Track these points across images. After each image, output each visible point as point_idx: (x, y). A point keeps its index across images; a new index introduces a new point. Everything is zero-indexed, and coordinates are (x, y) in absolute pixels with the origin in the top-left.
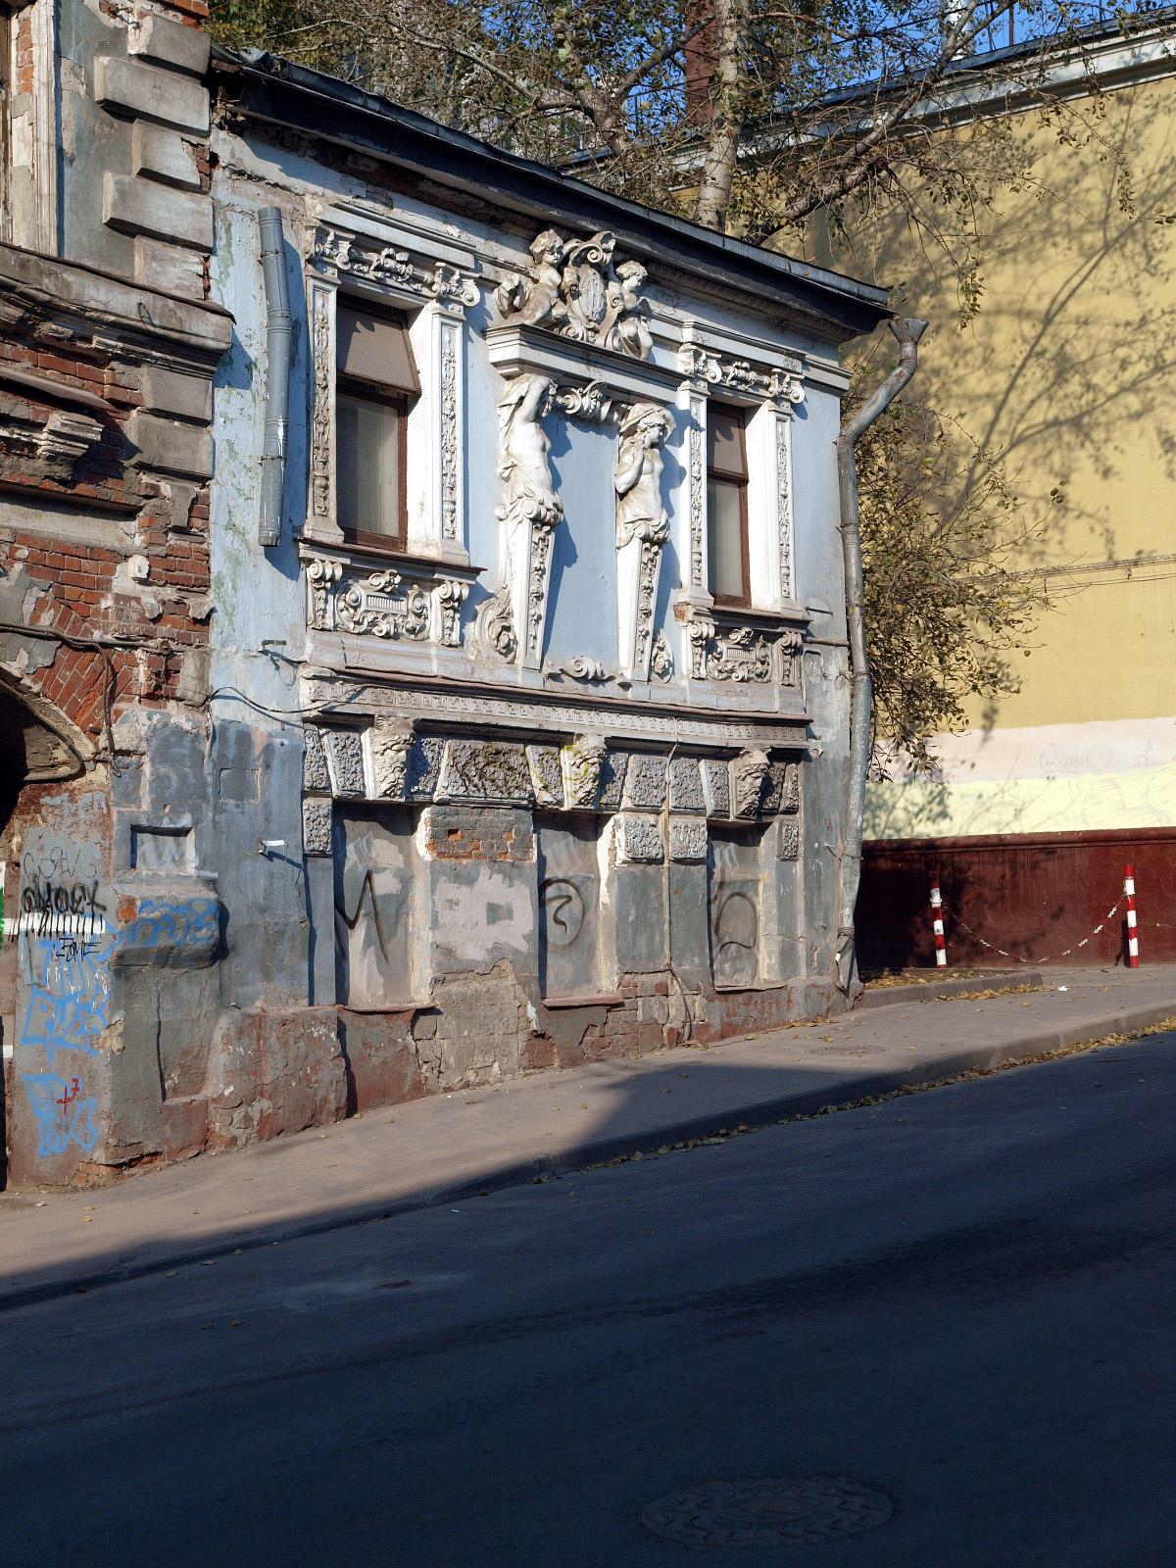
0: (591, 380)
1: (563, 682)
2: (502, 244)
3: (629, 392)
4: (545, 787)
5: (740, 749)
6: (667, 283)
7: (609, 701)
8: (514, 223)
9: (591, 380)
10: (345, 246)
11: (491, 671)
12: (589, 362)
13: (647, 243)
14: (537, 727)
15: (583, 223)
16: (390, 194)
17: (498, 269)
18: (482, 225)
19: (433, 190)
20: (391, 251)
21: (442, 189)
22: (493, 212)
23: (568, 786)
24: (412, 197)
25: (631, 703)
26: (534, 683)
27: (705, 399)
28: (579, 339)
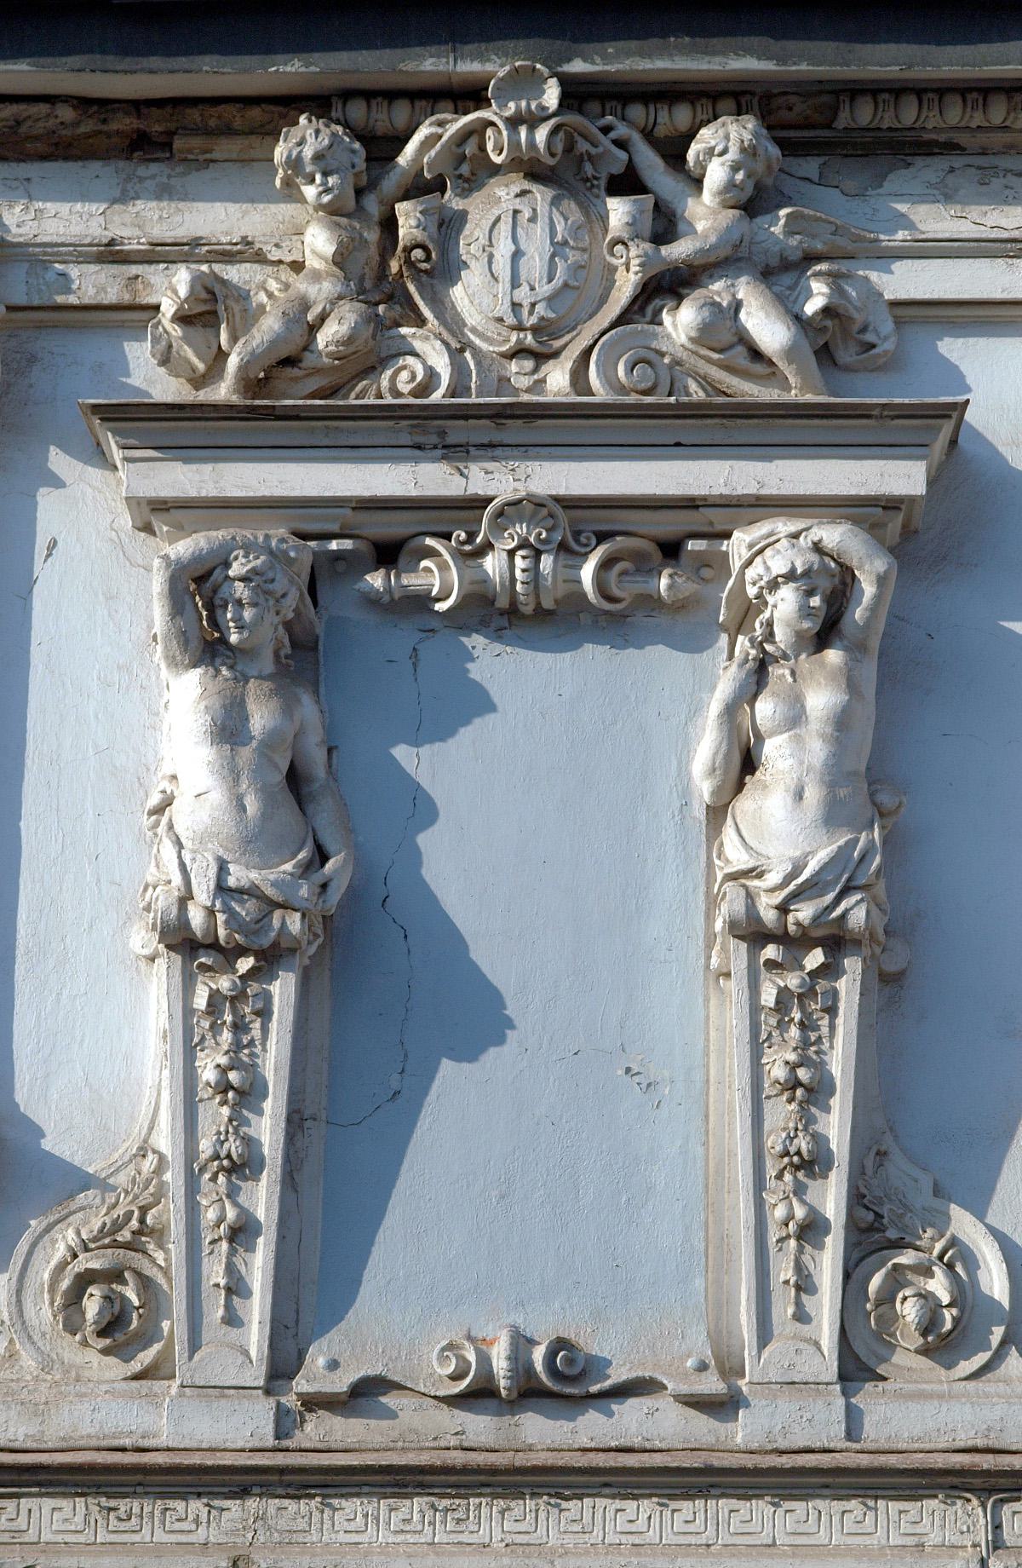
0: (490, 500)
1: (392, 1415)
2: (185, 198)
3: (691, 504)
6: (982, 139)
7: (986, 1462)
8: (228, 131)
9: (490, 500)
11: (38, 1411)
12: (455, 452)
13: (749, 51)
17: (134, 269)
18: (95, 166)
22: (124, 123)
25: (749, 1461)
28: (437, 397)
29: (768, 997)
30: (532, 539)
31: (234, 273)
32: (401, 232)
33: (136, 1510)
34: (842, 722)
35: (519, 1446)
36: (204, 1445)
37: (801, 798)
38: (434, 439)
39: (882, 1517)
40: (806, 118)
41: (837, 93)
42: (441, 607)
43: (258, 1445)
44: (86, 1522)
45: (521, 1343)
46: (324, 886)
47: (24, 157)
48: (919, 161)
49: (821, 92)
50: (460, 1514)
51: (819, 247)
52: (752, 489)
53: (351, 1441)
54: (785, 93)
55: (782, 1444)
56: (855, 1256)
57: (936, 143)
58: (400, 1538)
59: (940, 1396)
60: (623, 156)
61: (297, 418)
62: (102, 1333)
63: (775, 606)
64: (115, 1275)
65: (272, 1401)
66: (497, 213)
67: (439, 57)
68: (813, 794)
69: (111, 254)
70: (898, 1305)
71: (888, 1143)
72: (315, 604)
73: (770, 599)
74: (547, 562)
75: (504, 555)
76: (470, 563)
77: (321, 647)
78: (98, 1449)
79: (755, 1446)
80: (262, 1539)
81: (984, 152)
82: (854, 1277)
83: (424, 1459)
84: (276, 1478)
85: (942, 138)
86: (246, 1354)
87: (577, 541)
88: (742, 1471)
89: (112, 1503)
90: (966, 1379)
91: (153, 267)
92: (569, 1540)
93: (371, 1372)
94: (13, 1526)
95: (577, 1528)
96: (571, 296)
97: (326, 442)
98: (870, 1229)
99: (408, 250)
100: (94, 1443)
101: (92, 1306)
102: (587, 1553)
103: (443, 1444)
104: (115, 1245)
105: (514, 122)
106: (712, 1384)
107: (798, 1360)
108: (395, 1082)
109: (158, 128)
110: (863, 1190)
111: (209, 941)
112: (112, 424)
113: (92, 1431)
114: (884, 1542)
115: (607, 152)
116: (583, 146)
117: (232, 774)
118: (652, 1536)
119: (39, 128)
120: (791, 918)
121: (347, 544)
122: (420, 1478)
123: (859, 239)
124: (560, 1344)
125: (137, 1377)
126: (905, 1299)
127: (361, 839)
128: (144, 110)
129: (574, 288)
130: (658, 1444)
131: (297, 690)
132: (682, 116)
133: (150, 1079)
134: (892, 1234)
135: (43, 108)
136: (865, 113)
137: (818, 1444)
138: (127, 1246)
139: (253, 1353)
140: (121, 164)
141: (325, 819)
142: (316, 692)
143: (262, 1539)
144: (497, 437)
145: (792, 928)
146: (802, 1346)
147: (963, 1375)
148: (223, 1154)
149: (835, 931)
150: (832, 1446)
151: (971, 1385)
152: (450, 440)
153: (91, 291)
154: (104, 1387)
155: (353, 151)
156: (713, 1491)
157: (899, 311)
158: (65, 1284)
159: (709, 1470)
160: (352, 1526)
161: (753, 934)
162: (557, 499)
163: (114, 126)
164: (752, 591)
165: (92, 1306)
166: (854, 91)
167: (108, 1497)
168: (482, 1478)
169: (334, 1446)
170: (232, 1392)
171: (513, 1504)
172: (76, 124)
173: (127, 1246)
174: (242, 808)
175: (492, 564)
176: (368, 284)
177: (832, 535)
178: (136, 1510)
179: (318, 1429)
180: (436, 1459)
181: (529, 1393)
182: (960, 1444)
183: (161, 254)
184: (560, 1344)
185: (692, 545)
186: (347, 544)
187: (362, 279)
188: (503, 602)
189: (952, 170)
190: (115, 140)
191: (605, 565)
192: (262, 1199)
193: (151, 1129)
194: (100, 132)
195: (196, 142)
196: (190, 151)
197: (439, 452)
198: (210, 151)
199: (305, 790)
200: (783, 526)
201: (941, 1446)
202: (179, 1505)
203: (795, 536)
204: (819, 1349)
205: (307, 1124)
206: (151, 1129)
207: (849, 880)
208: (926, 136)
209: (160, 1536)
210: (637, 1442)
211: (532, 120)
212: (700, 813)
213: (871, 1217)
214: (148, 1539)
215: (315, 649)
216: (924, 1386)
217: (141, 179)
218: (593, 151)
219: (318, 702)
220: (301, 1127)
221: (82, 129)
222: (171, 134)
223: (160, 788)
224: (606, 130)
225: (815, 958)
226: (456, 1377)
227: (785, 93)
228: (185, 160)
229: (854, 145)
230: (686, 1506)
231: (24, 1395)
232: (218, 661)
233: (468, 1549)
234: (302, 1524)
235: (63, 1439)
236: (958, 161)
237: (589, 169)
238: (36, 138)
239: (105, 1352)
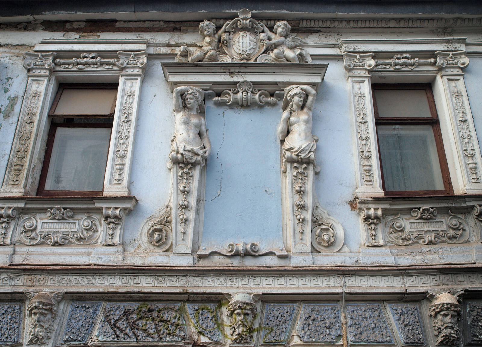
0: (239, 82)
3: (276, 84)
4: (200, 333)
5: (426, 293)
10: (51, 58)
11: (143, 258)
12: (231, 74)
14: (181, 291)
15: (227, 11)
16: (98, 34)
17: (173, 48)
18: (167, 33)
19: (126, 25)
20: (85, 54)
21: (131, 22)
23: (228, 331)
24: (114, 31)
26: (186, 262)
27: (367, 80)
29: (295, 174)
30: (246, 90)
31: (191, 49)
32: (222, 39)
33: (163, 279)
34: (307, 122)
35: (245, 266)
36: (178, 265)
37: (300, 135)
38: (228, 71)
39: (321, 281)
40: (294, 25)
41: (299, 20)
42: (228, 104)
43: (189, 265)
44: (153, 282)
45: (245, 244)
46: (205, 152)
47: (154, 31)
48: (314, 34)
49: (297, 20)
50: (232, 281)
51: (297, 44)
52: (288, 81)
53: (209, 265)
54: (291, 20)
55: (300, 265)
56: (313, 227)
57: (317, 30)
58: (219, 286)
59: (332, 255)
60: (262, 28)
61: (202, 66)
62: (157, 242)
63: (293, 101)
64: (160, 230)
65: (193, 257)
66: (239, 36)
67: (229, 9)
68: (303, 135)
69: (168, 45)
70: (323, 236)
71: (318, 205)
72: (205, 104)
73: (293, 100)
74: (249, 94)
75: (241, 93)
76: (234, 95)
77: (206, 112)
78: (156, 266)
79: (294, 266)
80: (190, 286)
81: (325, 32)
82: (313, 231)
83: (225, 268)
84: (193, 272)
85: (318, 29)
86: (188, 246)
87: (255, 90)
88: (292, 271)
89: (158, 278)
90: (336, 252)
91: (176, 48)
92: (255, 286)
93: (213, 250)
94: (137, 282)
95: (257, 283)
96: (253, 50)
97: (208, 71)
98: (315, 222)
99: (223, 42)
100: (155, 265)
101: (156, 237)
102: (259, 289)
103: (228, 265)
104: (161, 224)
105: (243, 19)
106: (284, 253)
107: (302, 248)
108: (219, 193)
109: (178, 26)
110: (314, 214)
111: (182, 162)
112: (167, 67)
113: (154, 263)
114: (322, 286)
115: (260, 27)
116: (255, 26)
117: (188, 131)
118: (273, 285)
119: (157, 26)
120: (299, 157)
121: (211, 91)
122: (224, 272)
123: (305, 43)
124: (253, 244)
125: (164, 252)
126: (324, 235)
127: (213, 146)
128: (176, 23)
129: (254, 49)
130: (274, 266)
131: (201, 118)
132: (272, 22)
133: (170, 192)
134: (320, 222)
135: (158, 22)
136: (304, 24)
137: (307, 265)
138: (164, 225)
139: (189, 247)
140: (172, 33)
141: (206, 142)
142: (204, 118)
143: (190, 286)
144: (240, 71)
145: (299, 159)
146: (303, 245)
147: (336, 251)
148: (184, 204)
149: (308, 161)
150: (310, 265)
151: (338, 253)
152: (231, 71)
153: (165, 52)
154: (158, 253)
155: (213, 26)
156: (286, 275)
157: (313, 57)
158: (151, 231)
159: (285, 270)
160: (209, 283)
161: (291, 161)
162: (252, 82)
163: (170, 26)
164: (289, 98)
165: (156, 237)
166: (303, 19)
167: (157, 277)
168: (237, 272)
169: (205, 266)
170: (184, 254)
171: (243, 278)
172: (163, 26)
173: (164, 225)
174: (189, 136)
175: (239, 95)
176: (216, 48)
177: (305, 87)
178: (163, 279)
179: (202, 263)
180: (227, 268)
181: (247, 254)
182: (337, 265)
183: (177, 45)
184: (253, 244)
185: (277, 92)
186: (211, 91)
187: (214, 47)
188: (240, 103)
189: (320, 35)
190: (171, 28)
191: (260, 96)
192: (191, 215)
193: (169, 202)
194: (168, 27)
195: (185, 28)
196: (184, 30)
197: (229, 74)
198: (187, 30)
199: (202, 137)
200: (295, 86)
201: (333, 265)
202: (173, 278)
203: (297, 87)
204: (307, 245)
205: (201, 201)
206: (169, 202)
207: (310, 150)
208: (316, 29)
209: (168, 285)
210: (270, 265)
211: (246, 19)
212: (279, 142)
213: (316, 219)
214: (166, 285)
215: (205, 113)
216: (328, 254)
217: (175, 35)
218: (257, 27)
219: (205, 120)
220: (200, 202)
221: (165, 26)
222: (180, 27)
223: (174, 135)
224: (259, 24)
225: (304, 166)
226: (231, 252)
227: (291, 20)
228: (183, 32)
229: (303, 30)
230: (280, 278)
231: (141, 255)
232: (186, 110)
233: (234, 288)
234: (198, 283)
235: (149, 264)
236: (321, 34)
237: (256, 30)
238: (156, 28)
239: (158, 246)
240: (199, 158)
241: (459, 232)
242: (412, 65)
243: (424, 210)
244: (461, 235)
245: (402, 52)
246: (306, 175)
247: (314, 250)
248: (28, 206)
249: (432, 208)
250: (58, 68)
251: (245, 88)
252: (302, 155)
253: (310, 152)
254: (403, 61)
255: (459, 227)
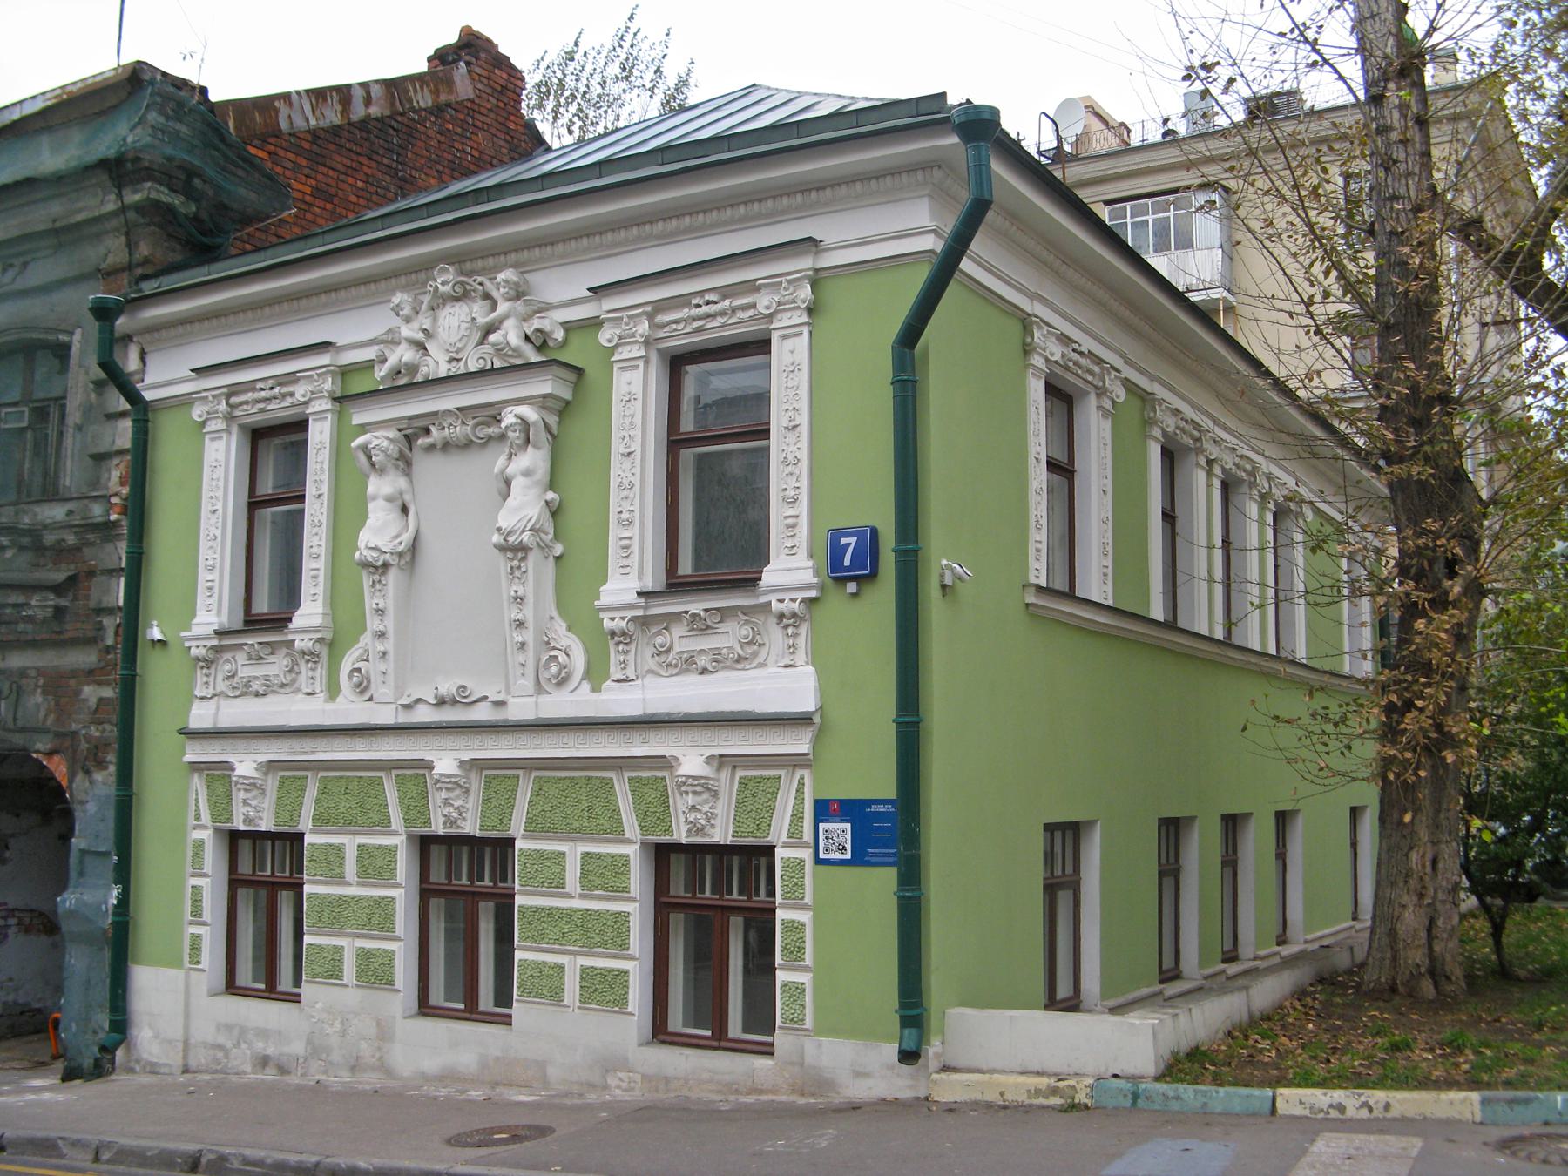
96: (465, 339)
161: (502, 548)
181: (454, 702)
225: (520, 555)
240: (387, 556)
241: (749, 650)
242: (722, 313)
243: (694, 615)
244: (755, 654)
245: (701, 293)
246: (523, 569)
247: (539, 689)
248: (225, 642)
249: (706, 610)
250: (237, 413)
251: (450, 420)
252: (511, 539)
253: (524, 531)
254: (705, 309)
255: (753, 638)
